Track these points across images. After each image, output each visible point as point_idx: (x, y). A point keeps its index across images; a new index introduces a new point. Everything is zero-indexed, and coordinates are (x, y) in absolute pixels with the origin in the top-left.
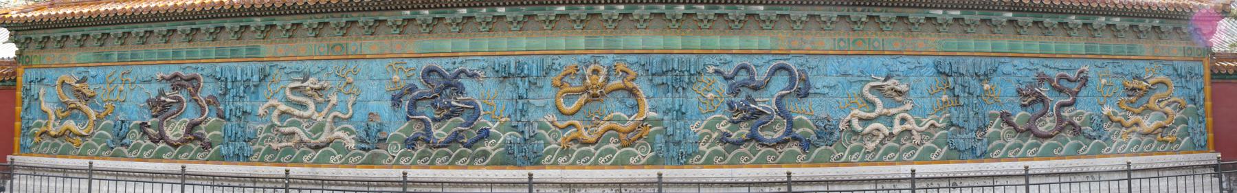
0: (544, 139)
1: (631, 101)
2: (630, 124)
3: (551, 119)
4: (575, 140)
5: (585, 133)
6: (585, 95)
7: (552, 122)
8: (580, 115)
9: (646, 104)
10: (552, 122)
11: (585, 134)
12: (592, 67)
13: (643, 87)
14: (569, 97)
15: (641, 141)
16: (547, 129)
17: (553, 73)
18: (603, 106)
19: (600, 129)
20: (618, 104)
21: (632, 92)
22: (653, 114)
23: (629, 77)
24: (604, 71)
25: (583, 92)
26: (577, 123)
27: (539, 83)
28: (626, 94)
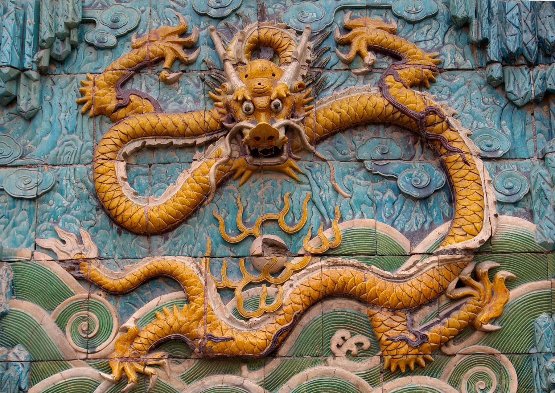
0: (32, 337)
1: (419, 173)
2: (417, 275)
3: (70, 249)
4: (173, 343)
5: (221, 312)
6: (224, 147)
7: (73, 265)
8: (202, 232)
9: (482, 188)
10: (73, 265)
11: (223, 323)
12: (252, 31)
13: (465, 112)
14: (156, 149)
15: (472, 345)
16: (50, 295)
17: (85, 59)
18: (300, 194)
19: (290, 292)
20: (362, 187)
21: (421, 134)
22: (514, 225)
23: (408, 72)
24: (298, 47)
25: (212, 133)
26: (183, 264)
27: (27, 99)
28: (393, 143)
